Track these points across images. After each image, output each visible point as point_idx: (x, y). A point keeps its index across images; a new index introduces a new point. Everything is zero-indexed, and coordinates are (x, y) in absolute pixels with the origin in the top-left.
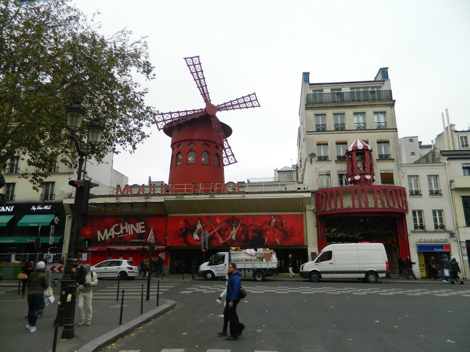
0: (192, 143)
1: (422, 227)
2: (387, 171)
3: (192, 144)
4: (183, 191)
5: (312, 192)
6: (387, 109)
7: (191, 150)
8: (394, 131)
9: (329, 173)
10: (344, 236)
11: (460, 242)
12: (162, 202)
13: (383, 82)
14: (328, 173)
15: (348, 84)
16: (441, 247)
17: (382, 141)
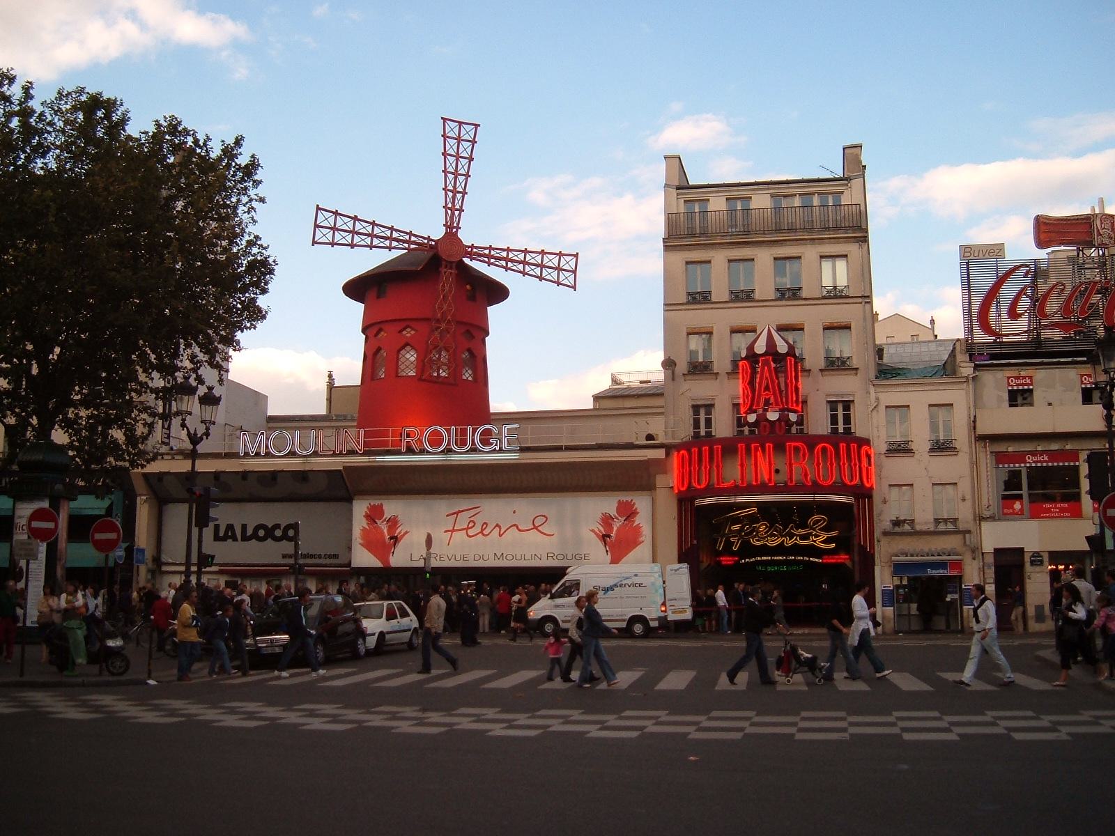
0: (408, 327)
2: (842, 396)
3: (409, 330)
4: (385, 444)
5: (668, 448)
6: (853, 249)
7: (407, 344)
8: (861, 303)
9: (712, 402)
11: (983, 554)
12: (340, 471)
13: (846, 182)
14: (709, 402)
15: (766, 186)
16: (942, 565)
17: (835, 325)
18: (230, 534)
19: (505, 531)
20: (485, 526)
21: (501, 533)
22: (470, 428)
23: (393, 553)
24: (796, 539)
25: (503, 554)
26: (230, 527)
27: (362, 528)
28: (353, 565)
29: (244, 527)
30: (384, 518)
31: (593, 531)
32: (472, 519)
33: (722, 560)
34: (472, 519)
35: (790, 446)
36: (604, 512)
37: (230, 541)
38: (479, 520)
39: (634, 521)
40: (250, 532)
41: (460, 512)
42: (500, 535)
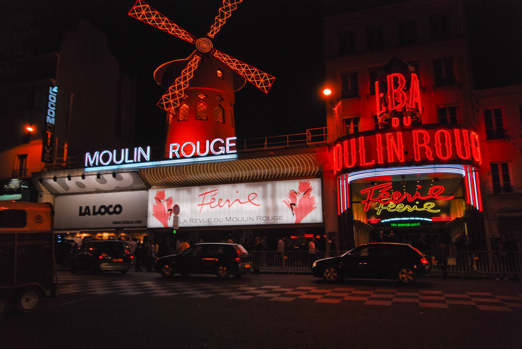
1: (508, 188)
10: (409, 210)
18: (87, 211)
19: (232, 203)
20: (220, 201)
21: (230, 204)
22: (208, 142)
23: (170, 219)
24: (415, 208)
25: (231, 218)
26: (87, 208)
27: (153, 205)
28: (148, 227)
29: (94, 207)
30: (165, 199)
31: (284, 202)
32: (213, 197)
33: (371, 221)
34: (213, 197)
35: (415, 133)
36: (291, 190)
37: (87, 215)
38: (217, 198)
39: (309, 195)
40: (97, 210)
41: (206, 193)
42: (229, 206)
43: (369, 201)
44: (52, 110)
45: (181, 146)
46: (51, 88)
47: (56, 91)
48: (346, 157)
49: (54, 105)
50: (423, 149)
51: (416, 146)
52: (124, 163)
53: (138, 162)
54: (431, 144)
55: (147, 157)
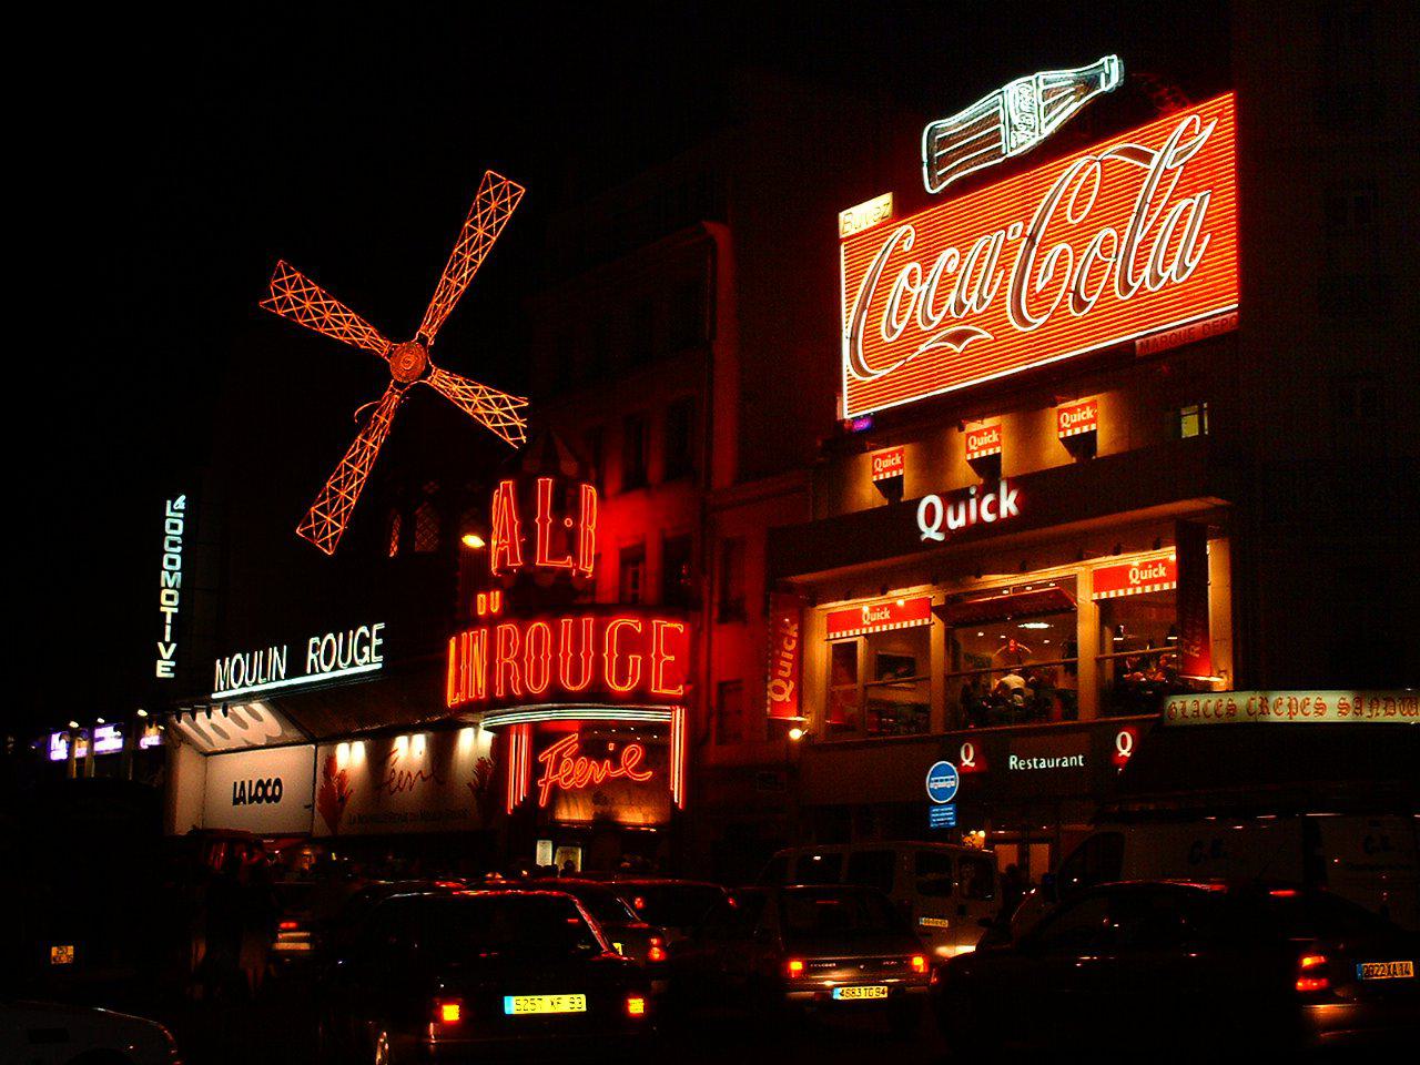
22: (351, 632)
26: (243, 783)
29: (251, 782)
43: (548, 779)
44: (173, 555)
45: (321, 641)
46: (169, 502)
47: (182, 507)
48: (545, 663)
49: (180, 542)
50: (508, 666)
51: (500, 661)
52: (256, 683)
53: (271, 681)
54: (519, 659)
55: (282, 672)
